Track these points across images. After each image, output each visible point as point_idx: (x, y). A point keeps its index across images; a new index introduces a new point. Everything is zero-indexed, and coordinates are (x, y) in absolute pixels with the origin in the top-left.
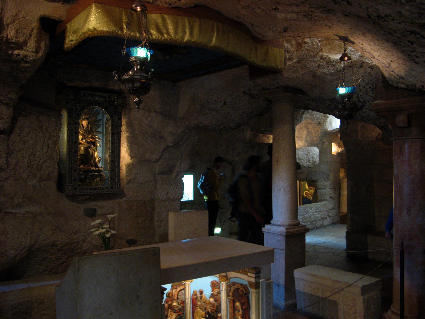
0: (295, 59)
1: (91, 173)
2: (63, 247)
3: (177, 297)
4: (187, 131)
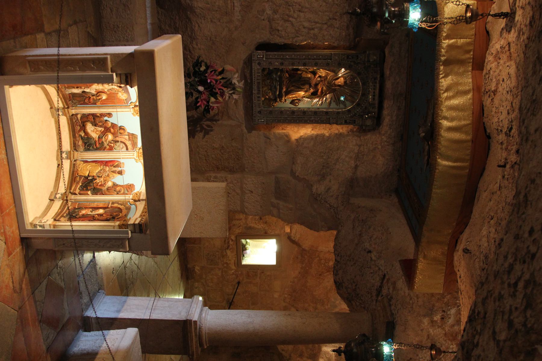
0: (433, 331)
2: (190, 52)
3: (118, 141)
4: (332, 210)
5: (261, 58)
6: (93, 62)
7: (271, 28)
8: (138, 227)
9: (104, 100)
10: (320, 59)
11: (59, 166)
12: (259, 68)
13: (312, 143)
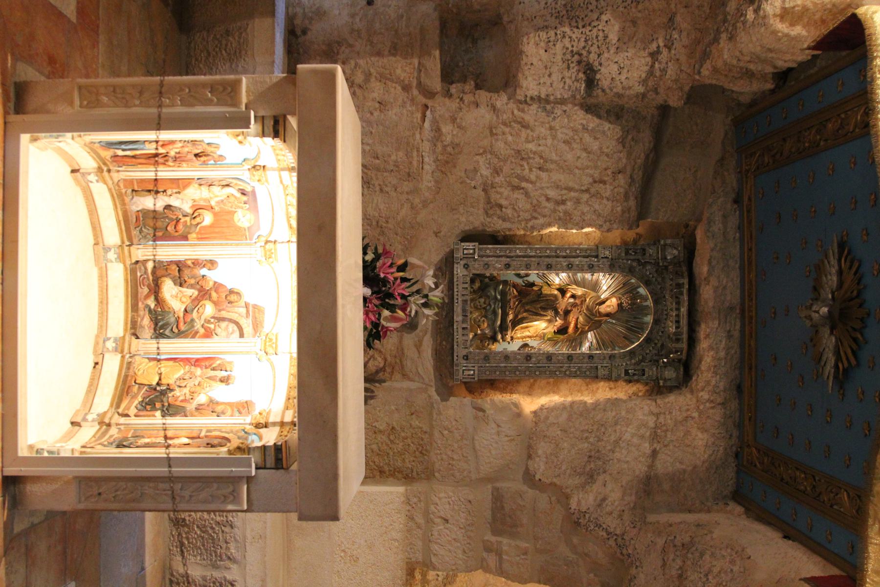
1: (500, 310)
3: (223, 319)
4: (612, 542)
5: (470, 254)
6: (212, 88)
7: (488, 202)
8: (272, 452)
9: (205, 227)
10: (578, 257)
11: (97, 366)
12: (466, 273)
13: (565, 415)
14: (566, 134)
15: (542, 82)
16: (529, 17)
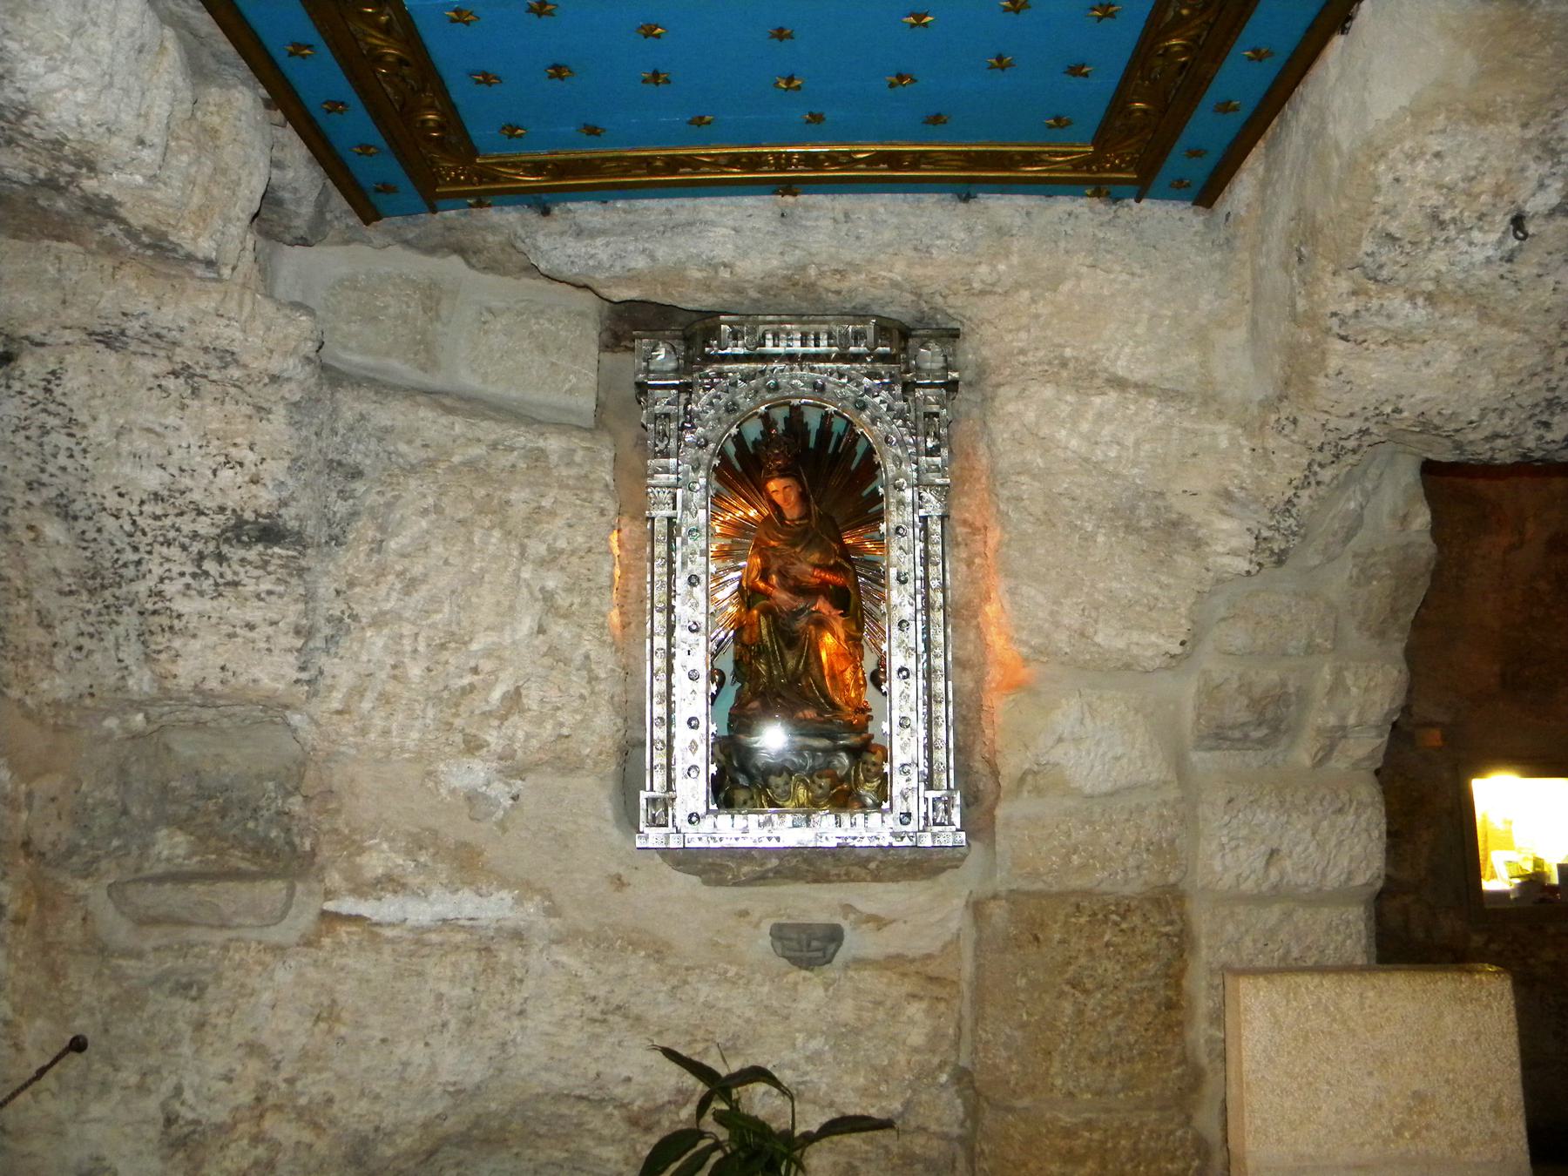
4: (1326, 475)
14: (391, 589)
15: (263, 645)
16: (118, 674)
